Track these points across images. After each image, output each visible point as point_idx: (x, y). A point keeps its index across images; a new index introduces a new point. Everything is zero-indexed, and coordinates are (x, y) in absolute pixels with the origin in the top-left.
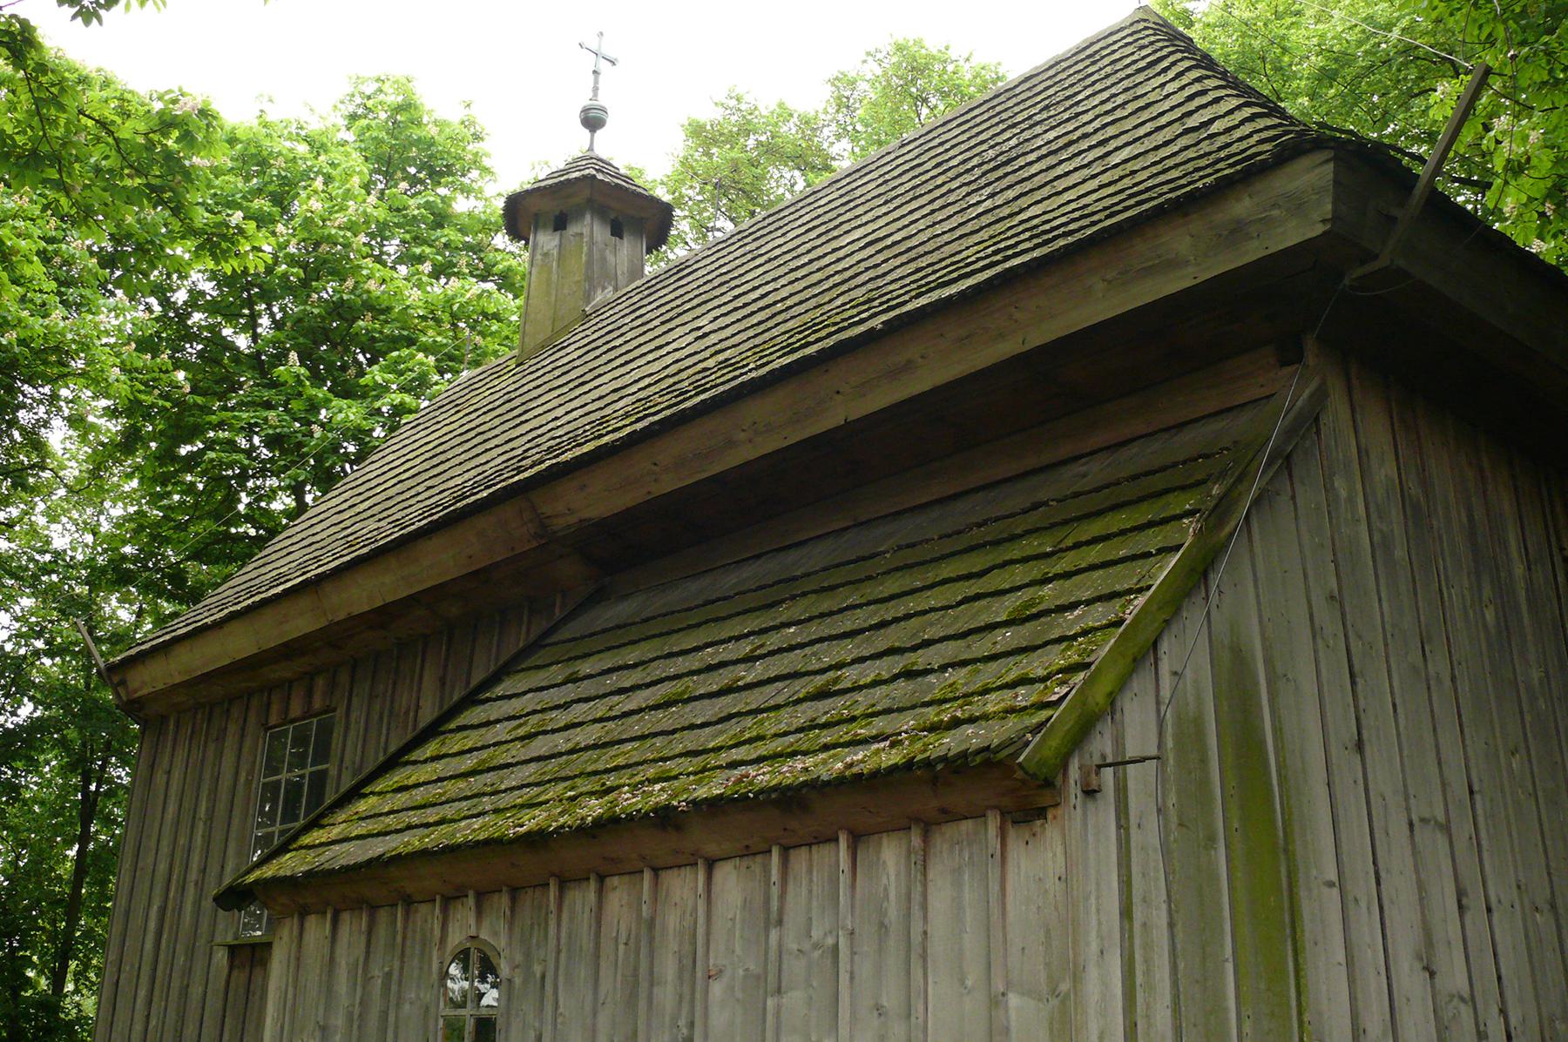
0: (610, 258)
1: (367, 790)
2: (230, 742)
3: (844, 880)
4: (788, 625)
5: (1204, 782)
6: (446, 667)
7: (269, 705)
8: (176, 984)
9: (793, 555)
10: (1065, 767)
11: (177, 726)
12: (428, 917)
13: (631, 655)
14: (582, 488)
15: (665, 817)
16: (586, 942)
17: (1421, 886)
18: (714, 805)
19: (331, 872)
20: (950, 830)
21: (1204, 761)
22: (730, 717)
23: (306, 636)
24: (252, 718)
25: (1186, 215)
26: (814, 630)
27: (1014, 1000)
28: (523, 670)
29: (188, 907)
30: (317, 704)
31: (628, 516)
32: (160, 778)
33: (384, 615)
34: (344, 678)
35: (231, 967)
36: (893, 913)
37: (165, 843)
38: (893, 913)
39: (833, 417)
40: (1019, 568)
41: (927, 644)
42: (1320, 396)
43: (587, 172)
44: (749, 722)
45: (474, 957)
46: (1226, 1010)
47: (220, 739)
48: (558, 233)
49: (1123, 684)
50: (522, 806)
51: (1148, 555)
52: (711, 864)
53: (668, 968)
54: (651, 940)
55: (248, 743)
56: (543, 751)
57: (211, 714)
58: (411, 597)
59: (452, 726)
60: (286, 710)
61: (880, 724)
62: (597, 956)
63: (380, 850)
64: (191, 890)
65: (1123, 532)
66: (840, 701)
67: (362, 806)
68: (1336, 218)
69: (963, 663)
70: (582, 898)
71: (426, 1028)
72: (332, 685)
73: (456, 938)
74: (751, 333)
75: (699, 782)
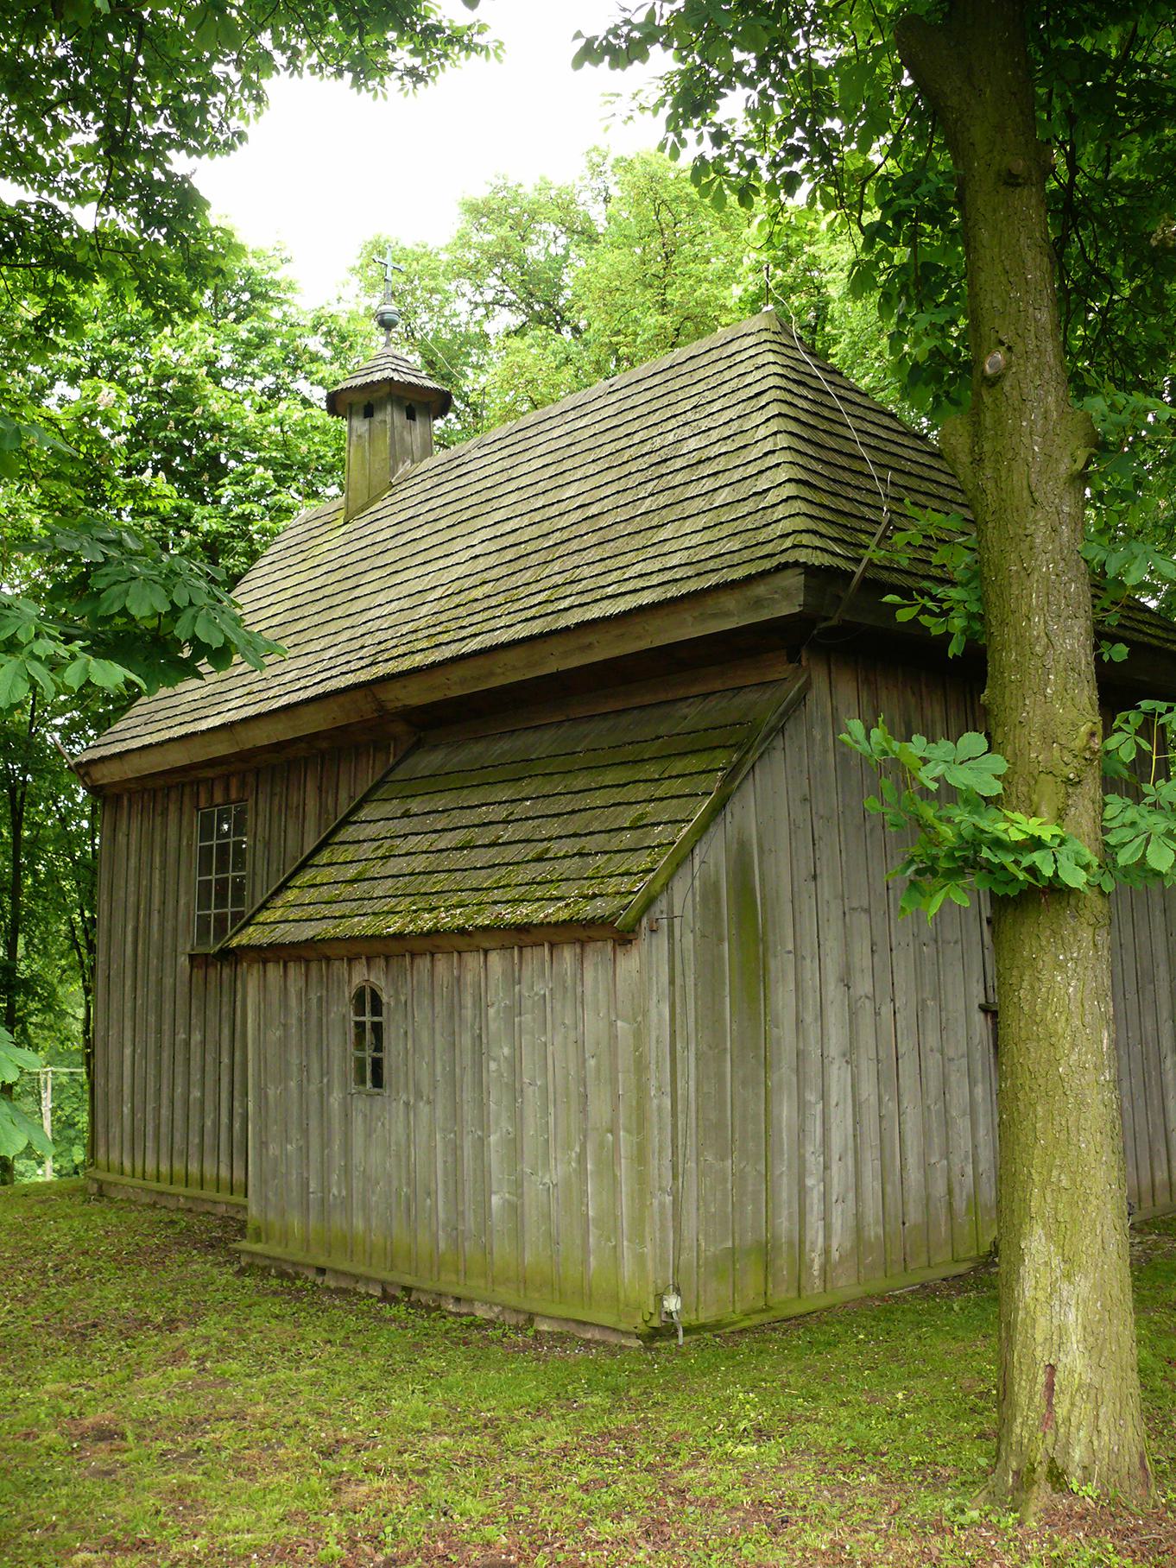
1: (291, 884)
3: (547, 965)
4: (527, 799)
5: (717, 916)
7: (198, 794)
8: (153, 978)
9: (530, 738)
10: (639, 921)
11: (129, 800)
12: (340, 968)
13: (440, 802)
14: (405, 687)
15: (462, 931)
18: (486, 928)
20: (592, 945)
21: (718, 902)
22: (494, 865)
24: (186, 800)
26: (542, 807)
27: (619, 1023)
29: (155, 928)
30: (234, 796)
31: (434, 705)
32: (121, 838)
33: (279, 747)
34: (251, 780)
35: (192, 968)
36: (569, 982)
37: (131, 882)
38: (569, 982)
39: (552, 666)
40: (642, 786)
42: (807, 686)
43: (387, 374)
44: (503, 871)
45: (368, 991)
46: (724, 1019)
47: (166, 810)
49: (671, 877)
50: (388, 913)
51: (697, 795)
52: (486, 952)
53: (468, 1001)
56: (394, 872)
59: (337, 840)
62: (433, 994)
64: (155, 917)
65: (691, 774)
66: (547, 866)
67: (291, 895)
68: (805, 605)
69: (606, 853)
70: (423, 963)
71: (344, 1027)
72: (243, 785)
73: (357, 980)
74: (503, 570)
75: (477, 912)
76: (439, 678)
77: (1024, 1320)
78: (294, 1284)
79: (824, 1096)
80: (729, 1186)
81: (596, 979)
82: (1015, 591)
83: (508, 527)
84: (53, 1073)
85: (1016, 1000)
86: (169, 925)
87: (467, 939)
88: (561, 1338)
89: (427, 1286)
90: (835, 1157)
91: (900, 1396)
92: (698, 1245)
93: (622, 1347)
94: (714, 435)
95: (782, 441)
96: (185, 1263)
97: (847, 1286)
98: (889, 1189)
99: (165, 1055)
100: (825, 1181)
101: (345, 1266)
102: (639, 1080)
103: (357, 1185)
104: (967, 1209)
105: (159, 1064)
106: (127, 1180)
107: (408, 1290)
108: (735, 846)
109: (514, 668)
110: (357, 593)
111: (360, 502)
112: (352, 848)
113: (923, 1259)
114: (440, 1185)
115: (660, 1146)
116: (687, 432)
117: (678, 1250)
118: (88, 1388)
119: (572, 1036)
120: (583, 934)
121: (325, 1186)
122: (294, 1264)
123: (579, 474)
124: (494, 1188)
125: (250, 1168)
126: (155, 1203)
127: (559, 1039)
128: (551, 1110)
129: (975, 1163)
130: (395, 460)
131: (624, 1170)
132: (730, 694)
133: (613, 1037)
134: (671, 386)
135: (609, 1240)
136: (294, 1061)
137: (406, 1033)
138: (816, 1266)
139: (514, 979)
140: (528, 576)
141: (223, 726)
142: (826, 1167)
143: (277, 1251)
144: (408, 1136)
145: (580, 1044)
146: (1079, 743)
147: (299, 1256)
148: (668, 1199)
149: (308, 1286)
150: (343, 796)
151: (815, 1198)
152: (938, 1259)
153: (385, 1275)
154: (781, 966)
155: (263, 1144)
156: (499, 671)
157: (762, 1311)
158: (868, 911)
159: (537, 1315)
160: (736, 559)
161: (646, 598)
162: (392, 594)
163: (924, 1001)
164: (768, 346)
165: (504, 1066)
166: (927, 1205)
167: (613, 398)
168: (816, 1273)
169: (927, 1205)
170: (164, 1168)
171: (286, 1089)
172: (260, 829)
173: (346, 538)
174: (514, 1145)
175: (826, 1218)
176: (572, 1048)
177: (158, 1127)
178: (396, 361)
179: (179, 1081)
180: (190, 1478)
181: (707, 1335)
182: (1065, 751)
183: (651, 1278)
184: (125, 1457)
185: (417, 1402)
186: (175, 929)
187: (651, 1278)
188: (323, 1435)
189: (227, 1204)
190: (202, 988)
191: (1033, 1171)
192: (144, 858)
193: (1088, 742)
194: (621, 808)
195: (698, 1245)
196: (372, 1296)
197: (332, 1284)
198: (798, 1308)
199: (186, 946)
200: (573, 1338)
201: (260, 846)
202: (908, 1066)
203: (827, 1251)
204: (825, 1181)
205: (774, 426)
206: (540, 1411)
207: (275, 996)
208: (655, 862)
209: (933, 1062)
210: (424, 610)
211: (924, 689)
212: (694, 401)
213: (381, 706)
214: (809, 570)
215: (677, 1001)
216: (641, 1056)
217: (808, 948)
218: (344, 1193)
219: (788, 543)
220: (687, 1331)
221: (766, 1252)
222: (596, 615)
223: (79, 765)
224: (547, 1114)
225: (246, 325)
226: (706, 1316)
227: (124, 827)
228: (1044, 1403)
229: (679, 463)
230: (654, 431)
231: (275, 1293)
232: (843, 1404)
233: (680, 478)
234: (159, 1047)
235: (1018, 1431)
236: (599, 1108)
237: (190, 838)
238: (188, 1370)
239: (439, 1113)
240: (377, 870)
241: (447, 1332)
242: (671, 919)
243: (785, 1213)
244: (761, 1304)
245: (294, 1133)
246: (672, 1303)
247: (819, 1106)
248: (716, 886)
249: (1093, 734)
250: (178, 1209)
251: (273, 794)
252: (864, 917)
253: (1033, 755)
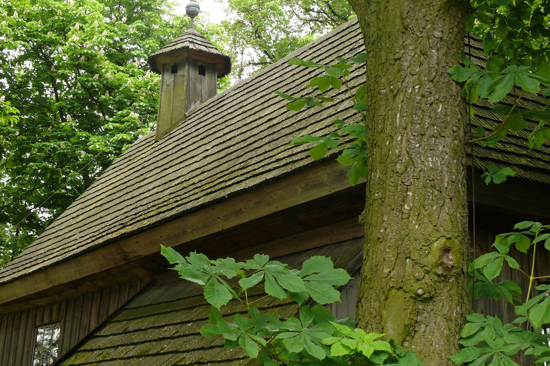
0: (197, 85)
4: (189, 322)
6: (100, 307)
23: (45, 290)
24: (30, 322)
25: (325, 166)
28: (114, 322)
30: (54, 319)
33: (74, 284)
34: (63, 307)
43: (186, 44)
48: (173, 74)
55: (28, 333)
57: (14, 317)
58: (83, 278)
59: (82, 349)
74: (216, 164)
82: (382, 112)
83: (228, 137)
111: (166, 128)
141: (40, 270)
146: (431, 259)
156: (189, 230)
173: (153, 150)
178: (194, 37)
182: (417, 267)
193: (440, 257)
222: (242, 188)
249: (446, 250)
253: (386, 271)
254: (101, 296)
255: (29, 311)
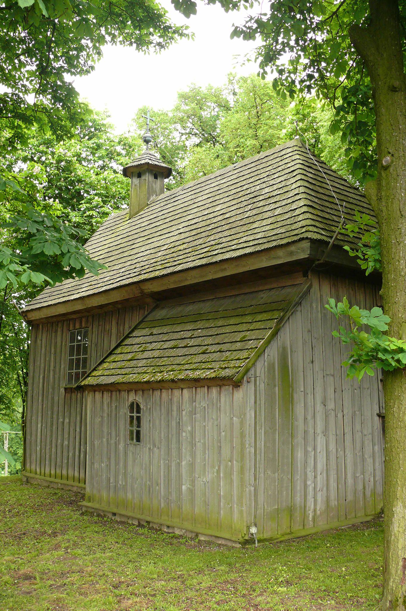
1: (105, 361)
2: (59, 333)
4: (199, 329)
5: (274, 375)
8: (50, 397)
9: (201, 305)
10: (243, 378)
12: (124, 394)
13: (165, 329)
15: (173, 381)
16: (158, 402)
17: (325, 389)
18: (182, 380)
19: (102, 385)
20: (224, 387)
21: (274, 371)
22: (186, 355)
26: (205, 332)
27: (234, 418)
29: (51, 376)
30: (83, 325)
32: (39, 342)
33: (101, 307)
34: (90, 319)
39: (210, 277)
41: (224, 343)
44: (190, 357)
45: (135, 404)
47: (56, 331)
49: (256, 361)
51: (266, 329)
52: (182, 389)
53: (175, 409)
54: (171, 403)
55: (64, 334)
60: (75, 326)
61: (213, 364)
63: (113, 381)
64: (52, 373)
65: (264, 320)
66: (206, 356)
67: (105, 365)
68: (310, 254)
69: (230, 351)
70: (157, 393)
71: (125, 418)
72: (87, 321)
73: (131, 399)
74: (191, 239)
75: (179, 373)
76: (165, 281)
77: (394, 540)
78: (103, 519)
79: (315, 449)
80: (277, 484)
81: (225, 401)
82: (394, 250)
84: (9, 433)
85: (392, 412)
86: (57, 376)
87: (174, 384)
88: (209, 543)
89: (156, 521)
90: (319, 473)
91: (344, 569)
92: (264, 507)
93: (233, 547)
94: (275, 187)
95: (302, 190)
96: (60, 510)
97: (323, 525)
98: (340, 486)
99: (54, 427)
100: (315, 482)
101: (123, 512)
102: (242, 441)
103: (129, 481)
104: (371, 495)
105: (51, 431)
106: (37, 476)
107: (148, 522)
108: (281, 349)
109: (195, 278)
110: (133, 247)
111: (136, 211)
112: (130, 347)
113: (353, 514)
114: (162, 481)
115: (250, 467)
116: (264, 185)
117: (256, 508)
118: (21, 559)
119: (216, 423)
120: (221, 383)
121: (116, 481)
122: (104, 511)
123: (222, 201)
124: (184, 483)
125: (87, 473)
126: (49, 486)
127: (210, 424)
128: (207, 452)
129: (374, 477)
130: (149, 195)
131: (235, 477)
132: (280, 289)
133: (232, 424)
134: (258, 167)
135: (229, 504)
136: (105, 430)
137: (150, 421)
138: (311, 516)
139: (193, 400)
140: (201, 241)
141: (80, 298)
142: (315, 477)
143: (96, 505)
144: (150, 461)
145: (218, 426)
147: (106, 508)
148: (252, 489)
149: (109, 520)
150: (127, 326)
151: (310, 489)
152: (359, 515)
153: (139, 516)
154: (298, 396)
155: (93, 463)
156: (189, 278)
157: (289, 534)
158: (333, 376)
159: (200, 533)
160: (283, 236)
161: (248, 251)
162: (148, 247)
163: (355, 412)
164: (297, 152)
165: (188, 435)
166: (355, 494)
167: (236, 172)
168: (310, 519)
169: (355, 494)
170: (53, 472)
171: (102, 442)
172: (93, 338)
173: (130, 225)
174: (192, 465)
175: (315, 498)
176: (215, 428)
177: (50, 456)
179: (60, 437)
180: (61, 596)
181: (267, 543)
183: (245, 520)
184: (35, 587)
185: (151, 567)
186: (59, 378)
187: (245, 520)
188: (114, 580)
189: (77, 487)
190: (69, 402)
191: (398, 480)
192: (48, 349)
194: (236, 333)
195: (264, 507)
196: (134, 525)
197: (119, 520)
198: (303, 533)
199: (63, 384)
200: (214, 543)
201: (93, 346)
202: (348, 437)
203: (315, 510)
204: (315, 482)
205: (298, 184)
206: (200, 572)
207: (98, 405)
208: (250, 355)
209: (358, 436)
210: (160, 254)
211: (356, 288)
212: (267, 173)
213: (142, 292)
214: (312, 241)
215: (257, 410)
216: (243, 431)
217: (309, 390)
218: (124, 483)
219: (304, 230)
220: (259, 541)
221: (291, 510)
223: (23, 312)
224: (205, 454)
225: (92, 141)
226: (266, 535)
227: (40, 336)
228: (402, 573)
229: (261, 198)
230: (251, 185)
231: (96, 523)
232: (321, 572)
233: (261, 204)
234: (52, 425)
235: (391, 584)
236: (226, 452)
237: (66, 342)
238: (61, 552)
239: (162, 453)
240: (140, 356)
241: (164, 540)
242: (256, 377)
243: (298, 495)
244: (288, 531)
245: (105, 460)
246: (253, 530)
247: (313, 453)
248: (274, 364)
250: (58, 488)
251: (99, 325)
252: (332, 378)
253: (400, 315)
254: (119, 312)
255: (64, 321)
